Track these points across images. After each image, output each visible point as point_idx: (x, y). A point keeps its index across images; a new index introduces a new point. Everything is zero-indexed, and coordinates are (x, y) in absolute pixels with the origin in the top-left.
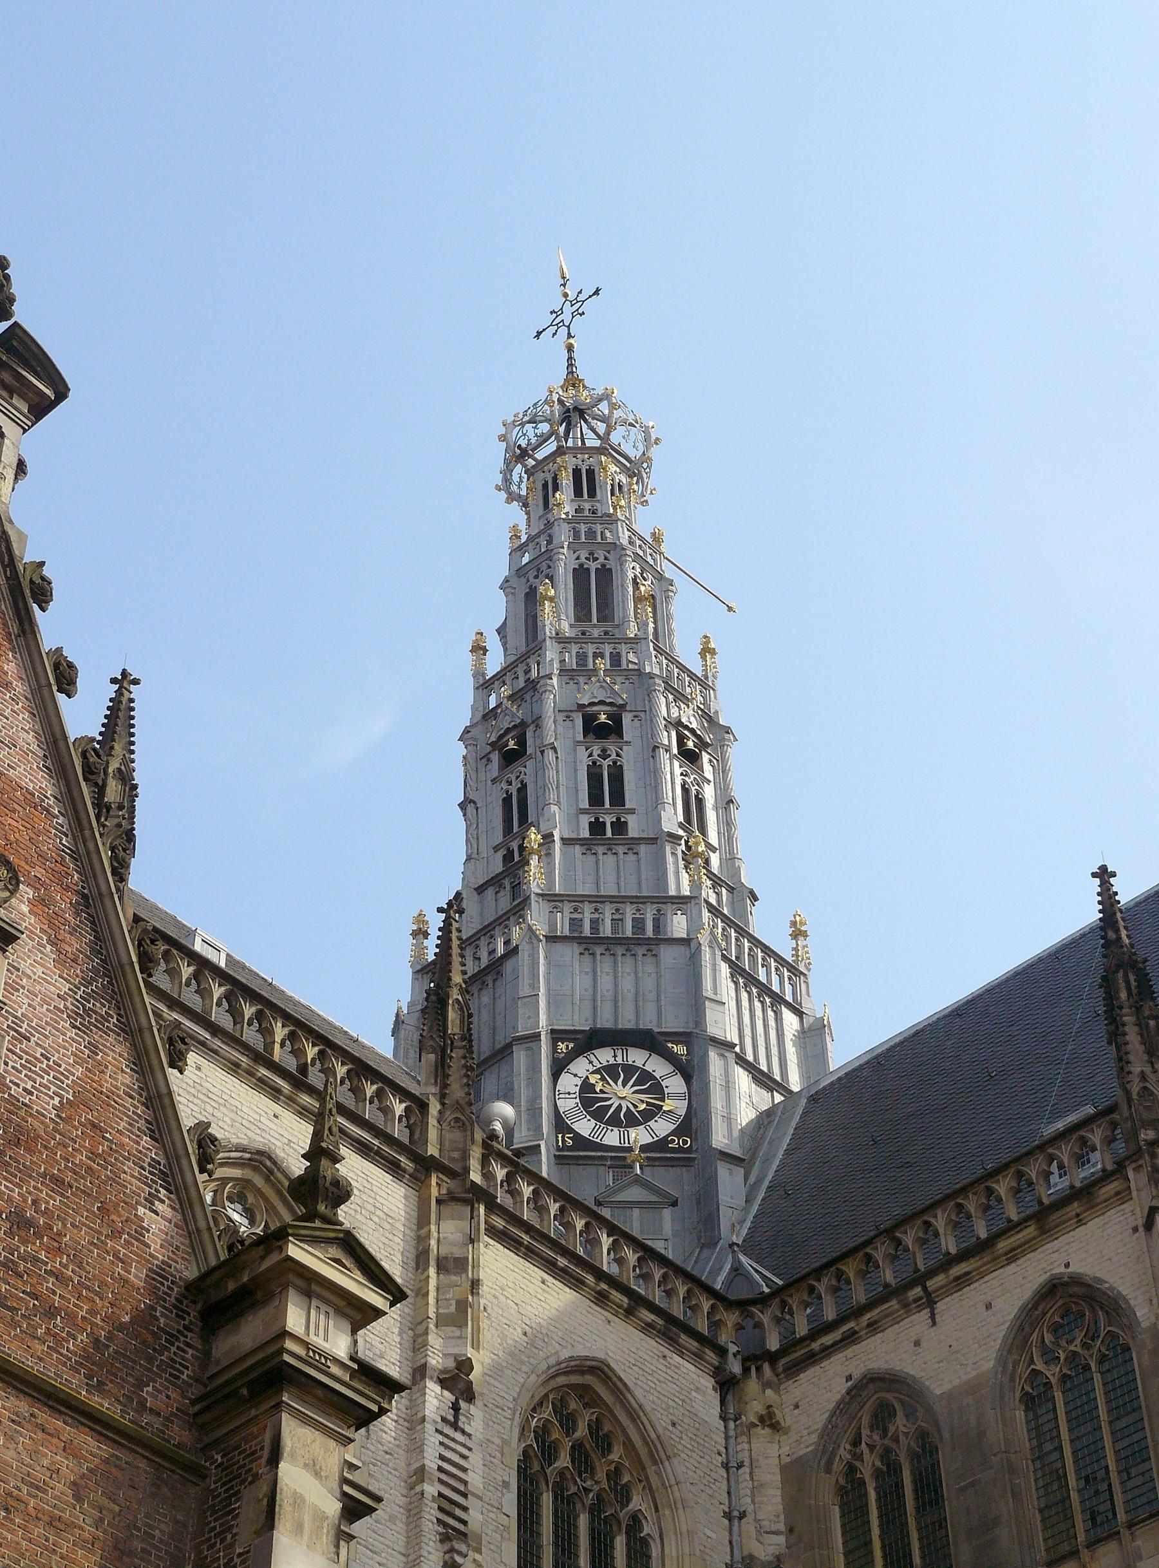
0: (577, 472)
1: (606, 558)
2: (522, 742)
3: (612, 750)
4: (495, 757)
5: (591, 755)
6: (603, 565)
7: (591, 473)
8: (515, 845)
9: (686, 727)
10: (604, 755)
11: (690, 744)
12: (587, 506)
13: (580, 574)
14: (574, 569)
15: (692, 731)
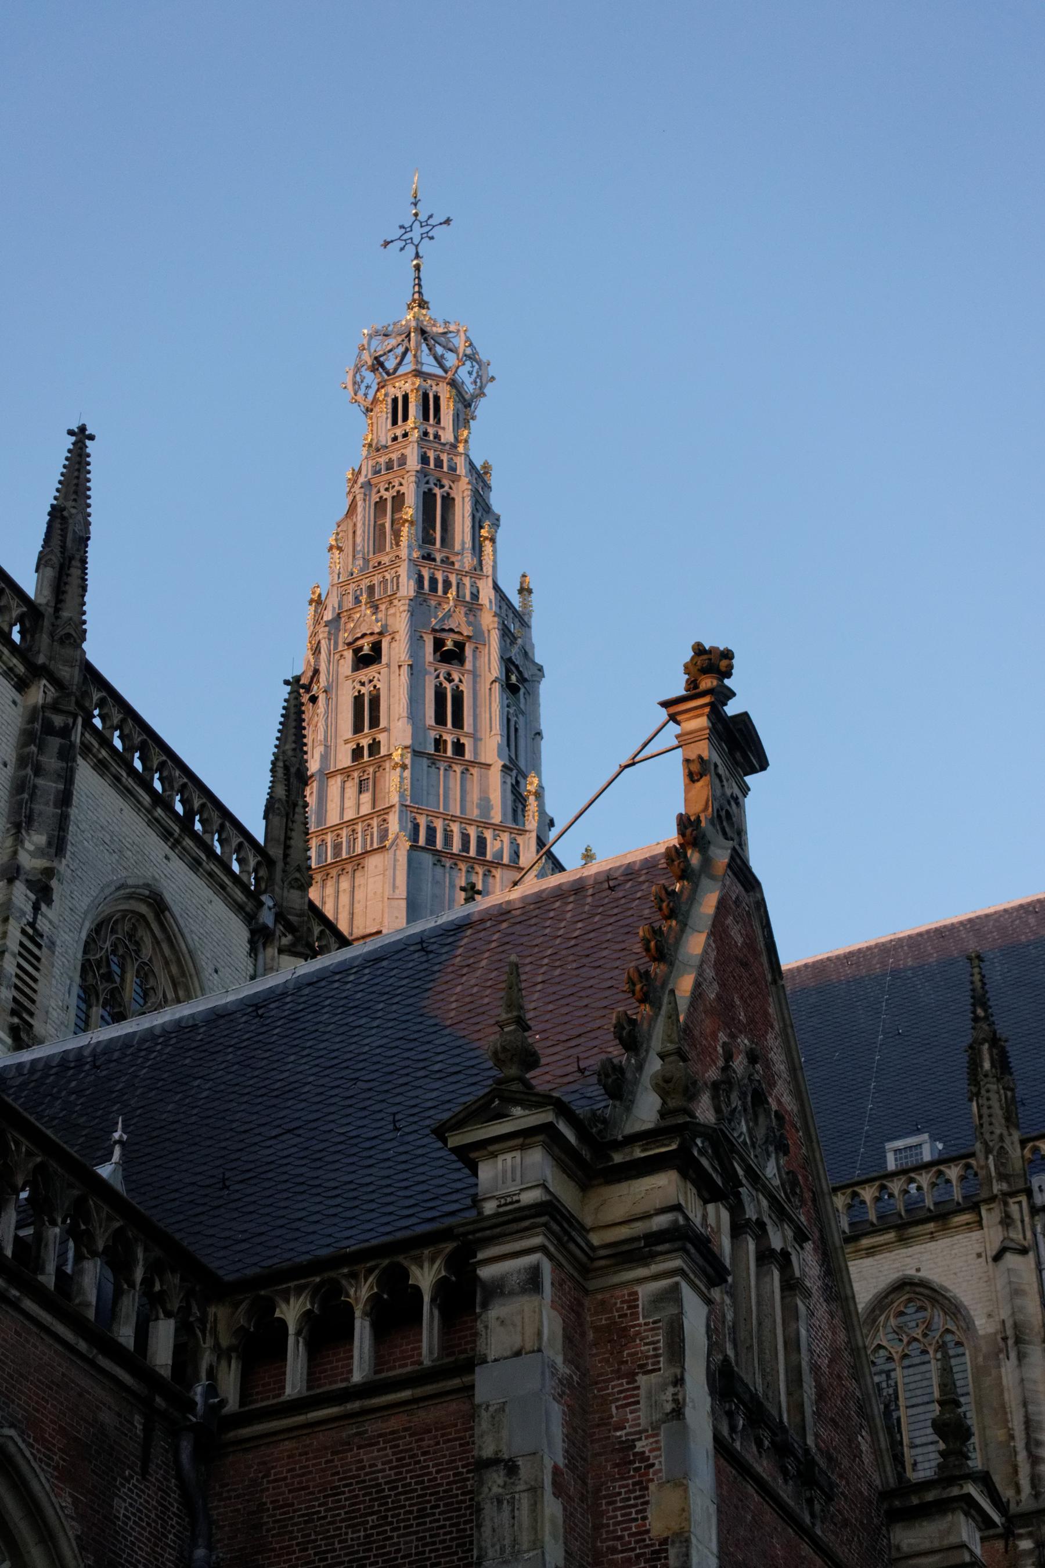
0: (425, 396)
1: (451, 488)
2: (377, 647)
3: (456, 676)
4: (349, 655)
5: (438, 677)
6: (448, 494)
7: (437, 399)
8: (365, 742)
9: (513, 663)
10: (450, 681)
11: (514, 678)
12: (431, 431)
13: (428, 499)
14: (424, 493)
15: (517, 667)
